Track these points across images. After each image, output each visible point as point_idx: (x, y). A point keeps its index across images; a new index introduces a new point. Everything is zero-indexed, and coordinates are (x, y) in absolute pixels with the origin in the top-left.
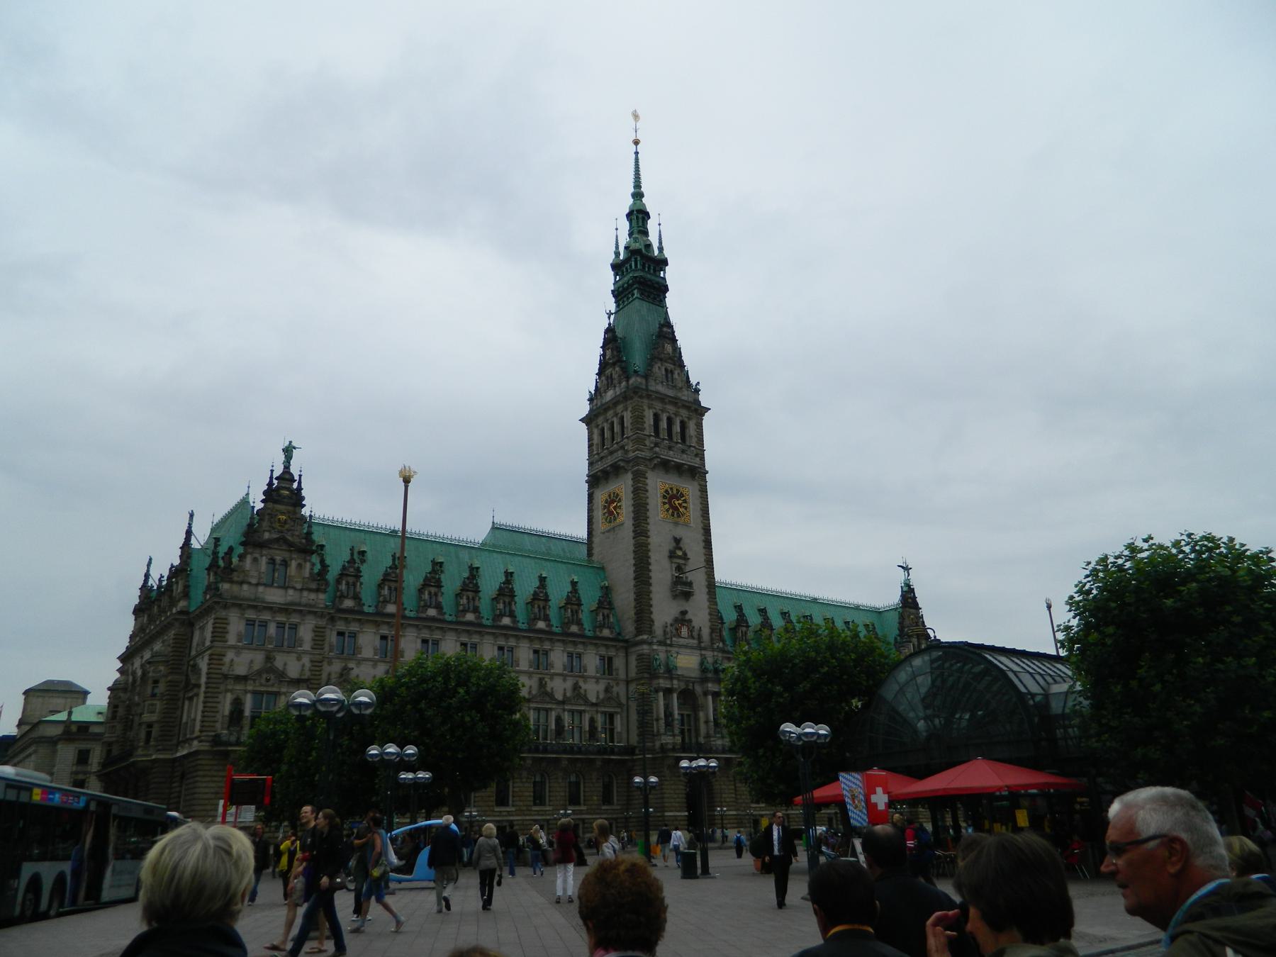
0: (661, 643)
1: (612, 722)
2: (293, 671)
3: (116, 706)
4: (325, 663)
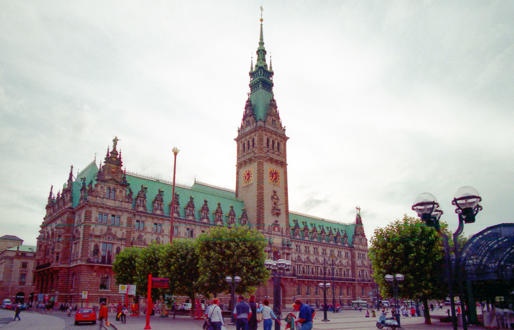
0: (267, 233)
2: (119, 235)
3: (41, 246)
4: (132, 233)
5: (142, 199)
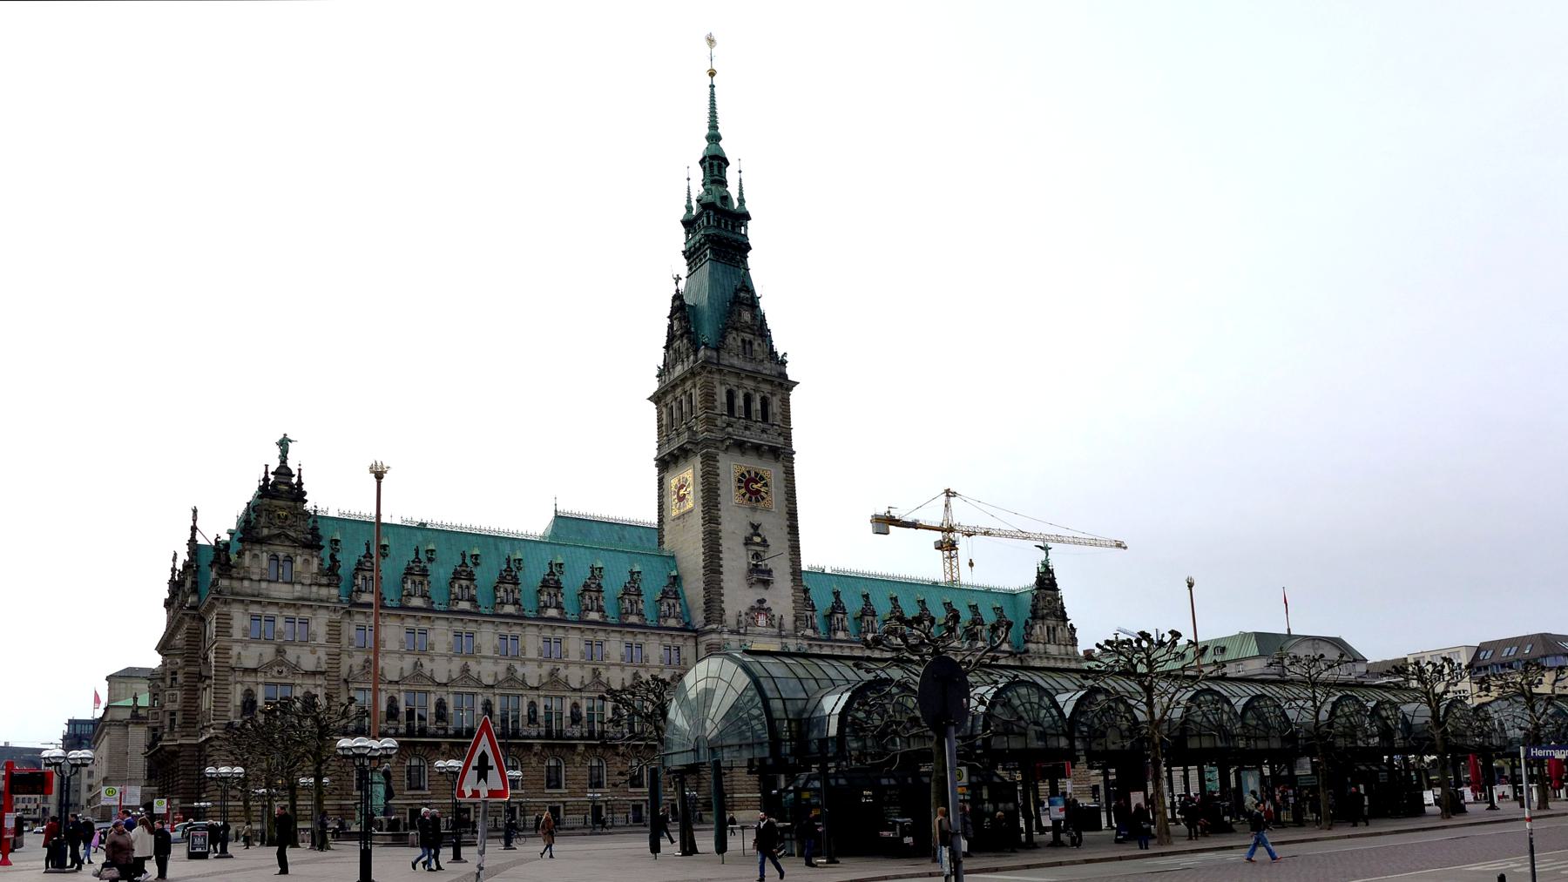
0: (732, 632)
4: (344, 657)
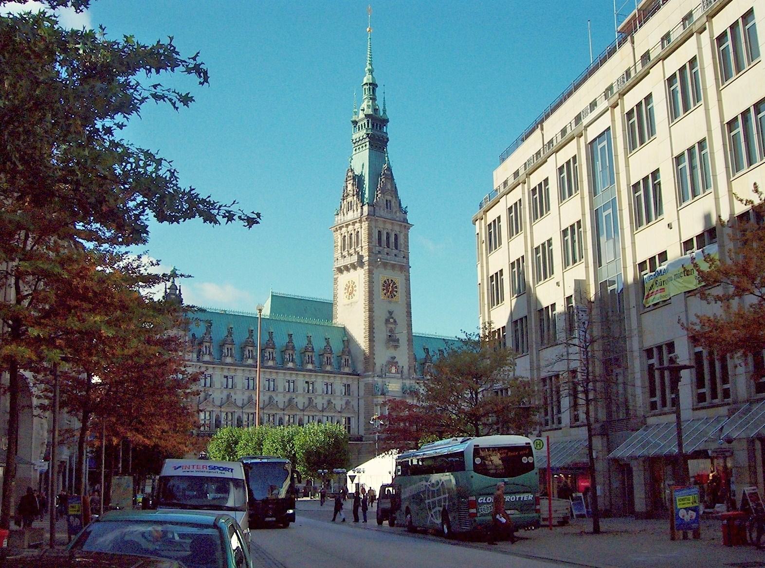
1: (349, 423)
5: (208, 344)
